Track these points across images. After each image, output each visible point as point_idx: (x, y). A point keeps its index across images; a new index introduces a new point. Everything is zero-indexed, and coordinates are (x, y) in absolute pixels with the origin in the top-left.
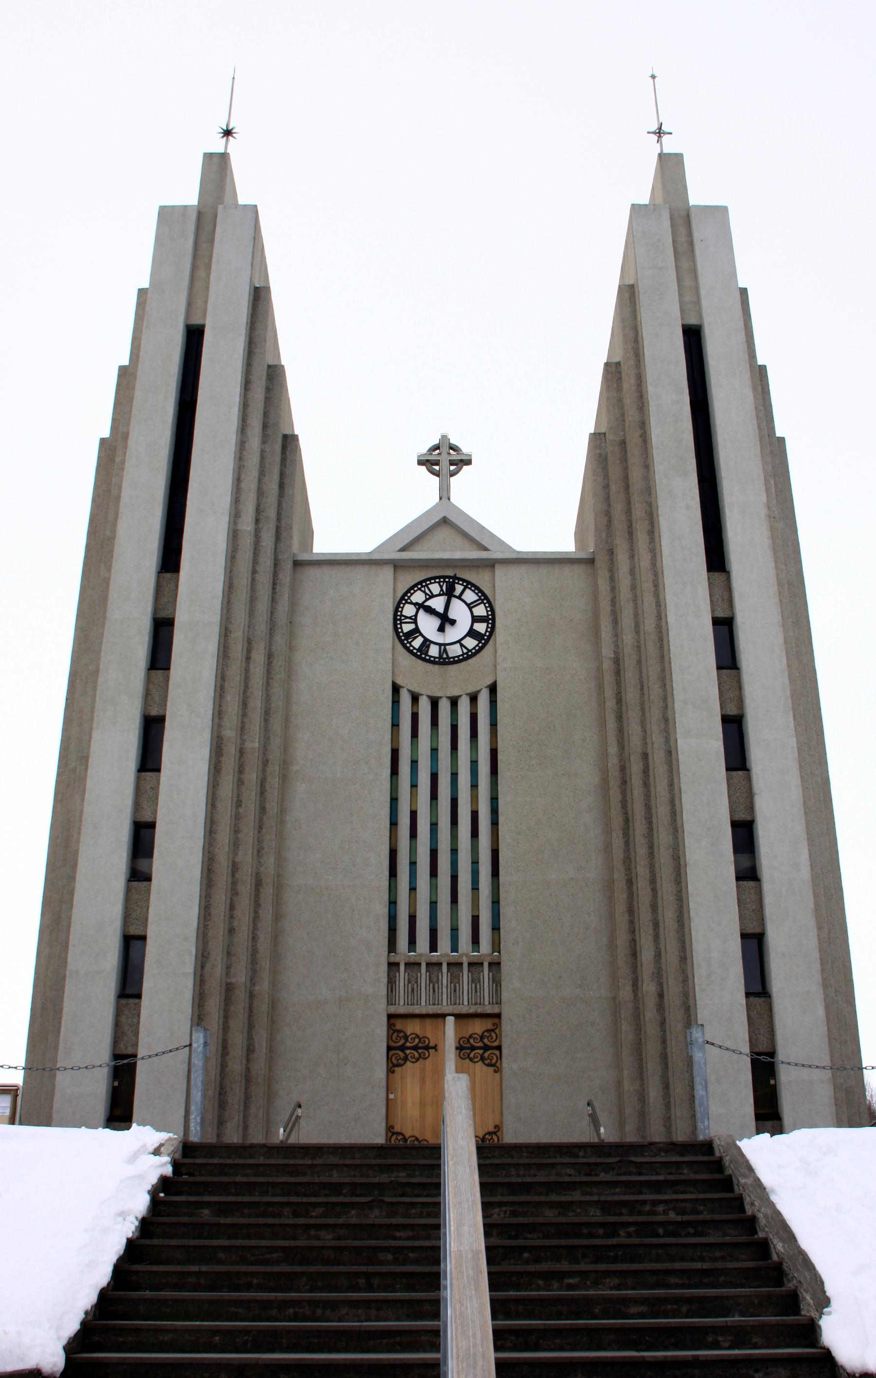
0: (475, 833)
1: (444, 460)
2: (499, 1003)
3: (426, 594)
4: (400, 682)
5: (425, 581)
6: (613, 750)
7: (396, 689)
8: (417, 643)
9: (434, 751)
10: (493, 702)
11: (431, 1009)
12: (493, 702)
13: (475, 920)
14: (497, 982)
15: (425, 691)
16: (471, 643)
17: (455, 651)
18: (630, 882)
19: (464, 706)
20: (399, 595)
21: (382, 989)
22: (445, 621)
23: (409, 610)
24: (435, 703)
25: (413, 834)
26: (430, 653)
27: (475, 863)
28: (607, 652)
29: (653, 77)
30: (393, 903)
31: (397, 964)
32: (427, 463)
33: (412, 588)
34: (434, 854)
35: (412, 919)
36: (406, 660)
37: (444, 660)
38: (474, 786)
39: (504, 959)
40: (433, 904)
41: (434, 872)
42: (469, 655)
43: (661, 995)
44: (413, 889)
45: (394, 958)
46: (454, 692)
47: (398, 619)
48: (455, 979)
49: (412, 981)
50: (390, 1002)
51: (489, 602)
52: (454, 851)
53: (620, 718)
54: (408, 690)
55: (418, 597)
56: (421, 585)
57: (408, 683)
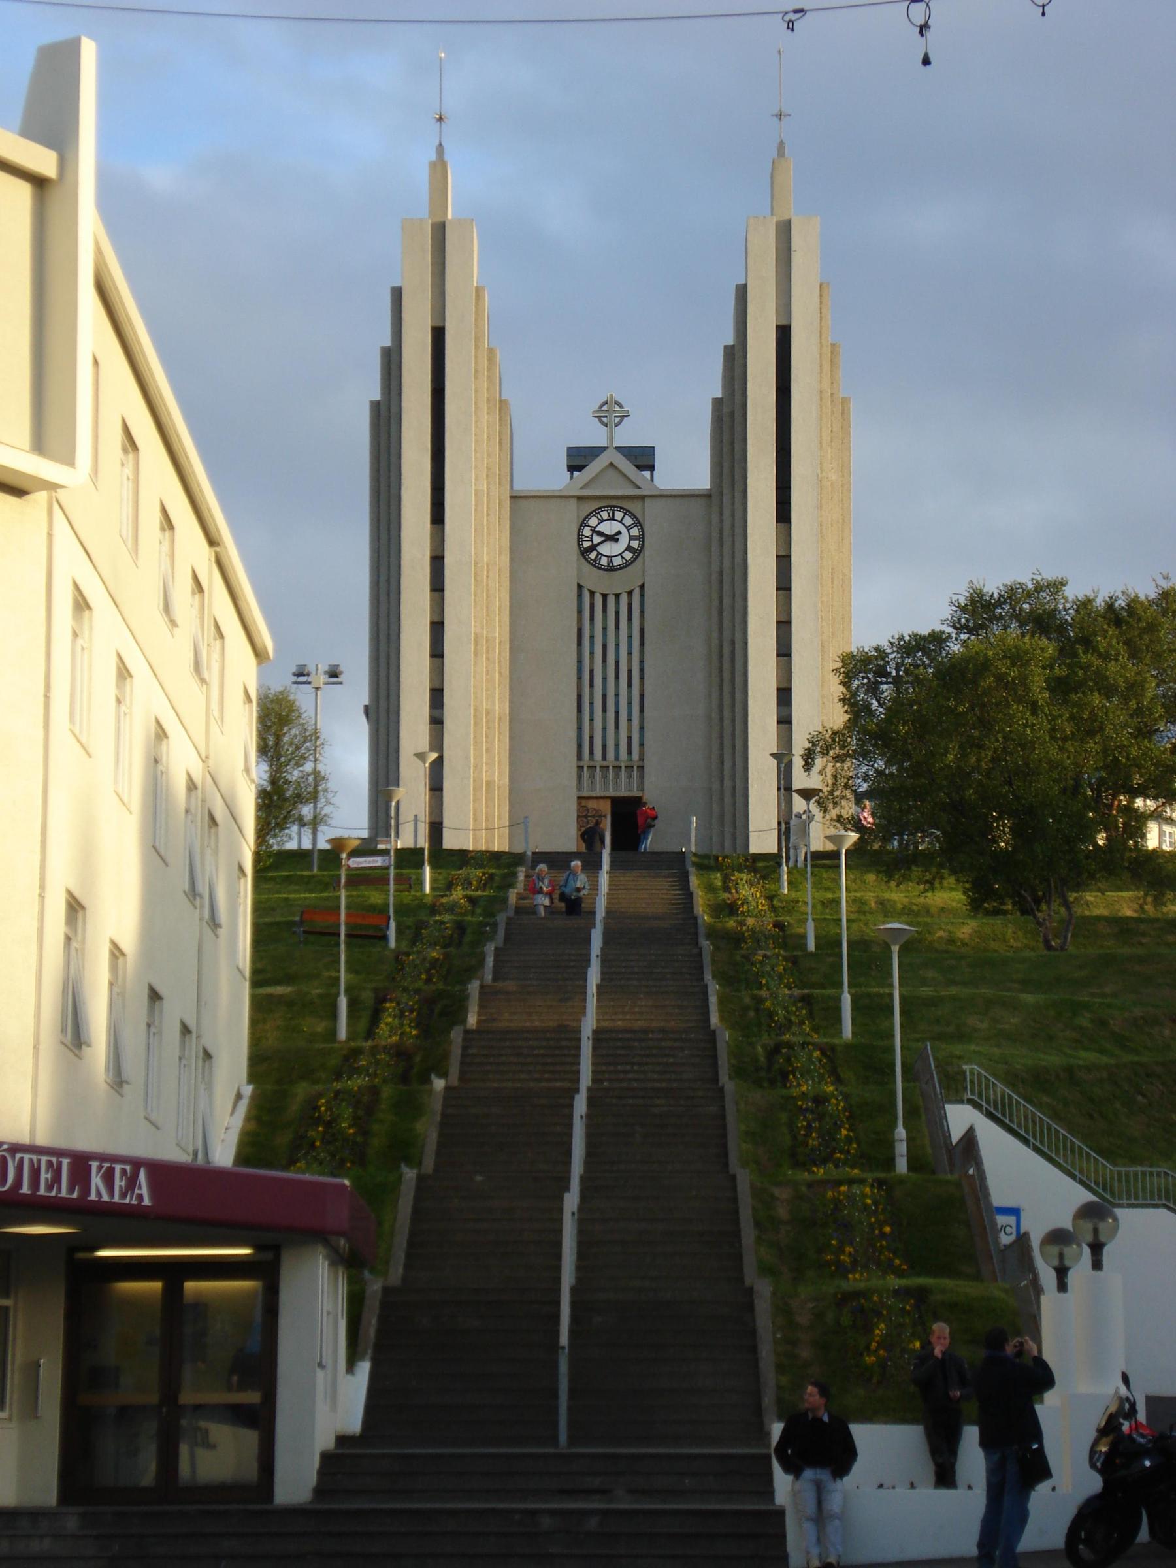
0: (630, 685)
2: (642, 790)
6: (715, 635)
7: (580, 587)
9: (605, 629)
10: (642, 595)
11: (602, 794)
12: (642, 595)
13: (630, 739)
14: (642, 777)
15: (599, 590)
16: (628, 556)
17: (617, 561)
18: (721, 719)
19: (624, 599)
21: (574, 782)
22: (614, 538)
23: (587, 532)
24: (605, 596)
25: (592, 685)
27: (630, 703)
28: (715, 567)
30: (580, 729)
31: (582, 767)
34: (604, 697)
35: (591, 738)
36: (587, 568)
37: (611, 568)
38: (630, 653)
39: (647, 764)
40: (604, 729)
41: (604, 710)
42: (627, 564)
43: (734, 788)
44: (592, 720)
45: (581, 764)
47: (580, 538)
48: (617, 776)
49: (592, 776)
50: (580, 789)
52: (617, 695)
53: (721, 613)
55: (593, 521)
56: (595, 512)
57: (588, 584)
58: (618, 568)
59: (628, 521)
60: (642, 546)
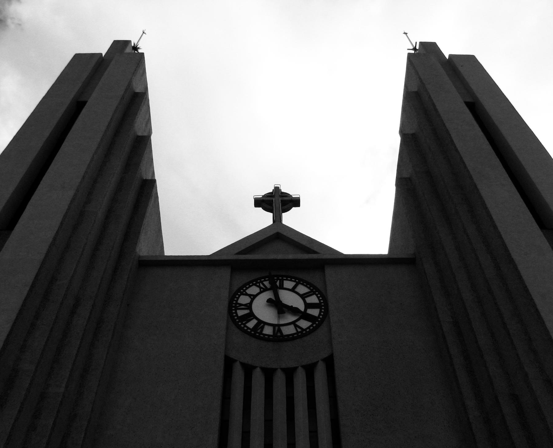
1: (277, 202)
3: (260, 288)
4: (233, 355)
5: (260, 279)
7: (229, 363)
8: (251, 324)
19: (300, 379)
20: (235, 289)
26: (264, 332)
29: (406, 33)
32: (262, 203)
33: (248, 283)
46: (291, 364)
47: (233, 305)
51: (320, 293)
54: (243, 365)
58: (291, 338)
59: (302, 289)
60: (325, 313)
